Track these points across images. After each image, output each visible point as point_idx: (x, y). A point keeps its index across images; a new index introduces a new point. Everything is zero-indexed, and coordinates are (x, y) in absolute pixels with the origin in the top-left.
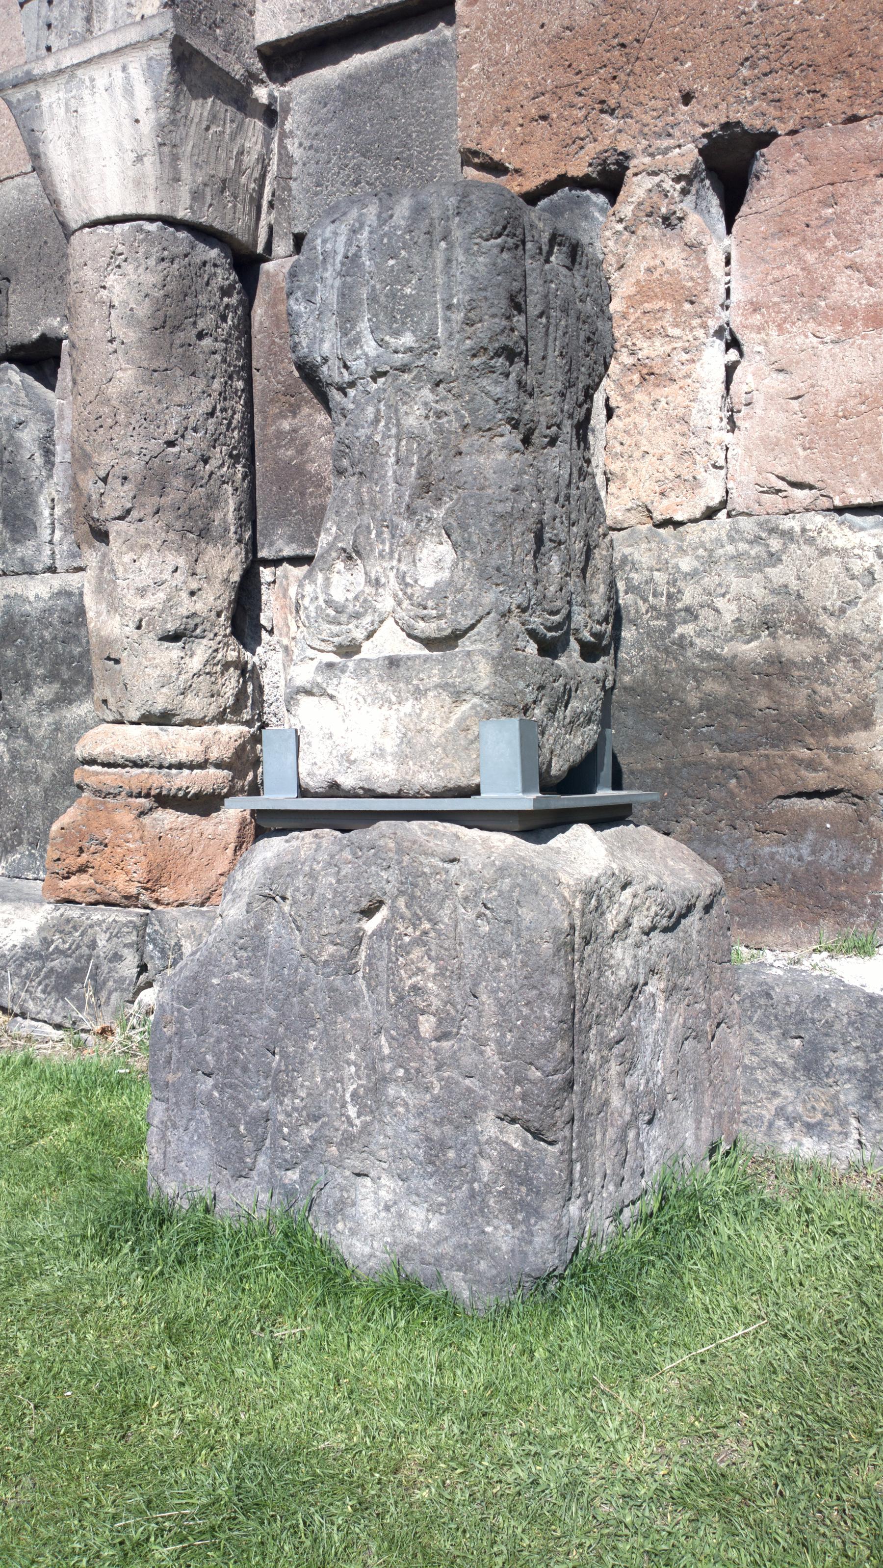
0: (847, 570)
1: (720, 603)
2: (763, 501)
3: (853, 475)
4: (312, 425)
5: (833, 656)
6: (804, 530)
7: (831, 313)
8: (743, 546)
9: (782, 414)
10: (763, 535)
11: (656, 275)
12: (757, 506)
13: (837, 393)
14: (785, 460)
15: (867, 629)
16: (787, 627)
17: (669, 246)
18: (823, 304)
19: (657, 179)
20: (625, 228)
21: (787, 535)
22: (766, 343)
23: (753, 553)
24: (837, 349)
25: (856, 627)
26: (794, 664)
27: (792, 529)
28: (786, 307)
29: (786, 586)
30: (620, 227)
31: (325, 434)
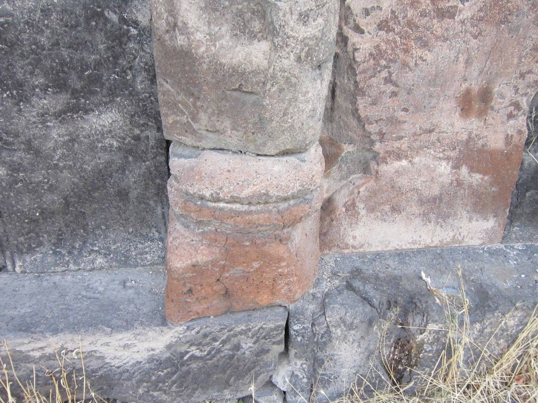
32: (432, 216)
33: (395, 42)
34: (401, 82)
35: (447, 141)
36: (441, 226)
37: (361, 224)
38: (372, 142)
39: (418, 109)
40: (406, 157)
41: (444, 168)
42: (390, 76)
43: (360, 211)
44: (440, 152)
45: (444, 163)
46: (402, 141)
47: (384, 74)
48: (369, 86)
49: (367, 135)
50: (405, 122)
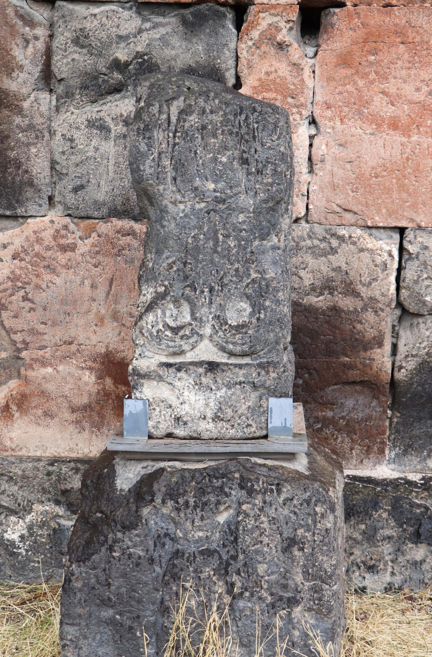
0: (373, 261)
1: (302, 273)
2: (328, 217)
3: (379, 211)
4: (11, 123)
5: (365, 309)
6: (350, 237)
7: (370, 117)
8: (316, 242)
9: (341, 171)
10: (328, 237)
11: (272, 77)
12: (324, 220)
13: (371, 163)
14: (342, 197)
15: (383, 295)
16: (339, 290)
17: (280, 61)
18: (366, 111)
19: (276, 19)
20: (254, 44)
21: (341, 239)
22: (333, 128)
23: (322, 246)
24: (372, 138)
25: (377, 294)
26: (344, 311)
27: (344, 235)
28: (346, 109)
29: (340, 267)
30: (250, 43)
31: (22, 132)
32: (87, 425)
33: (28, 269)
34: (37, 300)
35: (86, 353)
36: (97, 435)
37: (16, 425)
38: (19, 350)
39: (55, 324)
40: (51, 365)
41: (89, 378)
42: (27, 295)
43: (13, 413)
44: (82, 362)
45: (87, 373)
46: (46, 351)
47: (22, 293)
48: (11, 303)
49: (14, 343)
50: (45, 334)
